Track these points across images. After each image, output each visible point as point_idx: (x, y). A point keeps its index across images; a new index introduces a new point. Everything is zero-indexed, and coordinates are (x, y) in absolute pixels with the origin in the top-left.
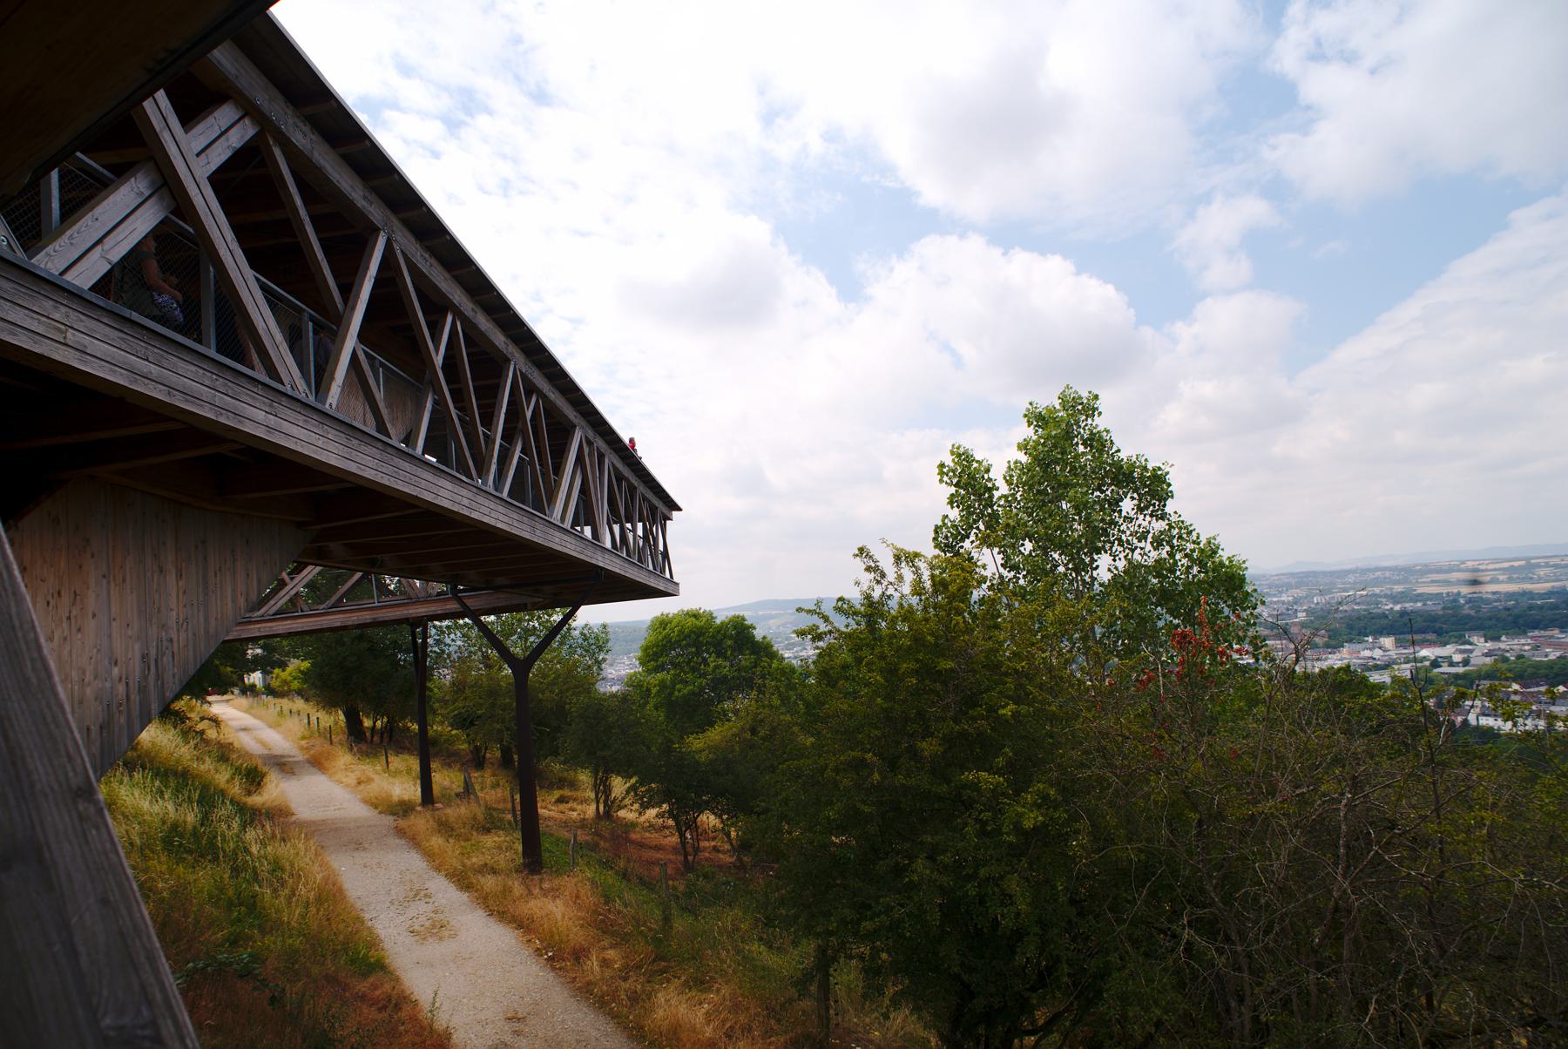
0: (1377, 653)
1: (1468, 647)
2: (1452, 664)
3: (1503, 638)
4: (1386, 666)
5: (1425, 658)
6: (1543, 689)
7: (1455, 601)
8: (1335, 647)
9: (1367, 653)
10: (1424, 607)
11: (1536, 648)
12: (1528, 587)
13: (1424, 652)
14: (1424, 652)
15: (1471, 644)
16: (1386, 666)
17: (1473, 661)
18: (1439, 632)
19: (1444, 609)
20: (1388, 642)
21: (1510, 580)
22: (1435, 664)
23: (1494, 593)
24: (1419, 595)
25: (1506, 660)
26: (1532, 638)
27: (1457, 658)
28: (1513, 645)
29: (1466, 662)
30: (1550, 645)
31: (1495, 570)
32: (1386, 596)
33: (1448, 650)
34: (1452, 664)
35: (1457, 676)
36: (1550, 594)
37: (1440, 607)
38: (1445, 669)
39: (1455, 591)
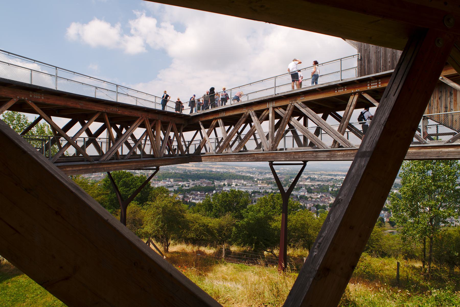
0: (170, 183)
1: (189, 182)
2: (186, 187)
3: (195, 181)
4: (172, 186)
5: (180, 185)
6: (204, 193)
7: (185, 171)
8: (159, 181)
9: (167, 183)
10: (179, 172)
11: (201, 183)
12: (199, 169)
13: (180, 183)
14: (180, 183)
15: (189, 182)
16: (172, 186)
17: (190, 186)
18: (183, 178)
19: (184, 173)
20: (172, 180)
21: (196, 167)
22: (182, 186)
23: (193, 170)
24: (178, 168)
25: (196, 186)
26: (201, 181)
27: (187, 185)
28: (198, 182)
29: (188, 186)
30: (204, 183)
31: (193, 164)
32: (170, 168)
33: (184, 183)
34: (186, 187)
35: (187, 189)
36: (203, 171)
37: (183, 172)
38: (184, 188)
39: (185, 168)
